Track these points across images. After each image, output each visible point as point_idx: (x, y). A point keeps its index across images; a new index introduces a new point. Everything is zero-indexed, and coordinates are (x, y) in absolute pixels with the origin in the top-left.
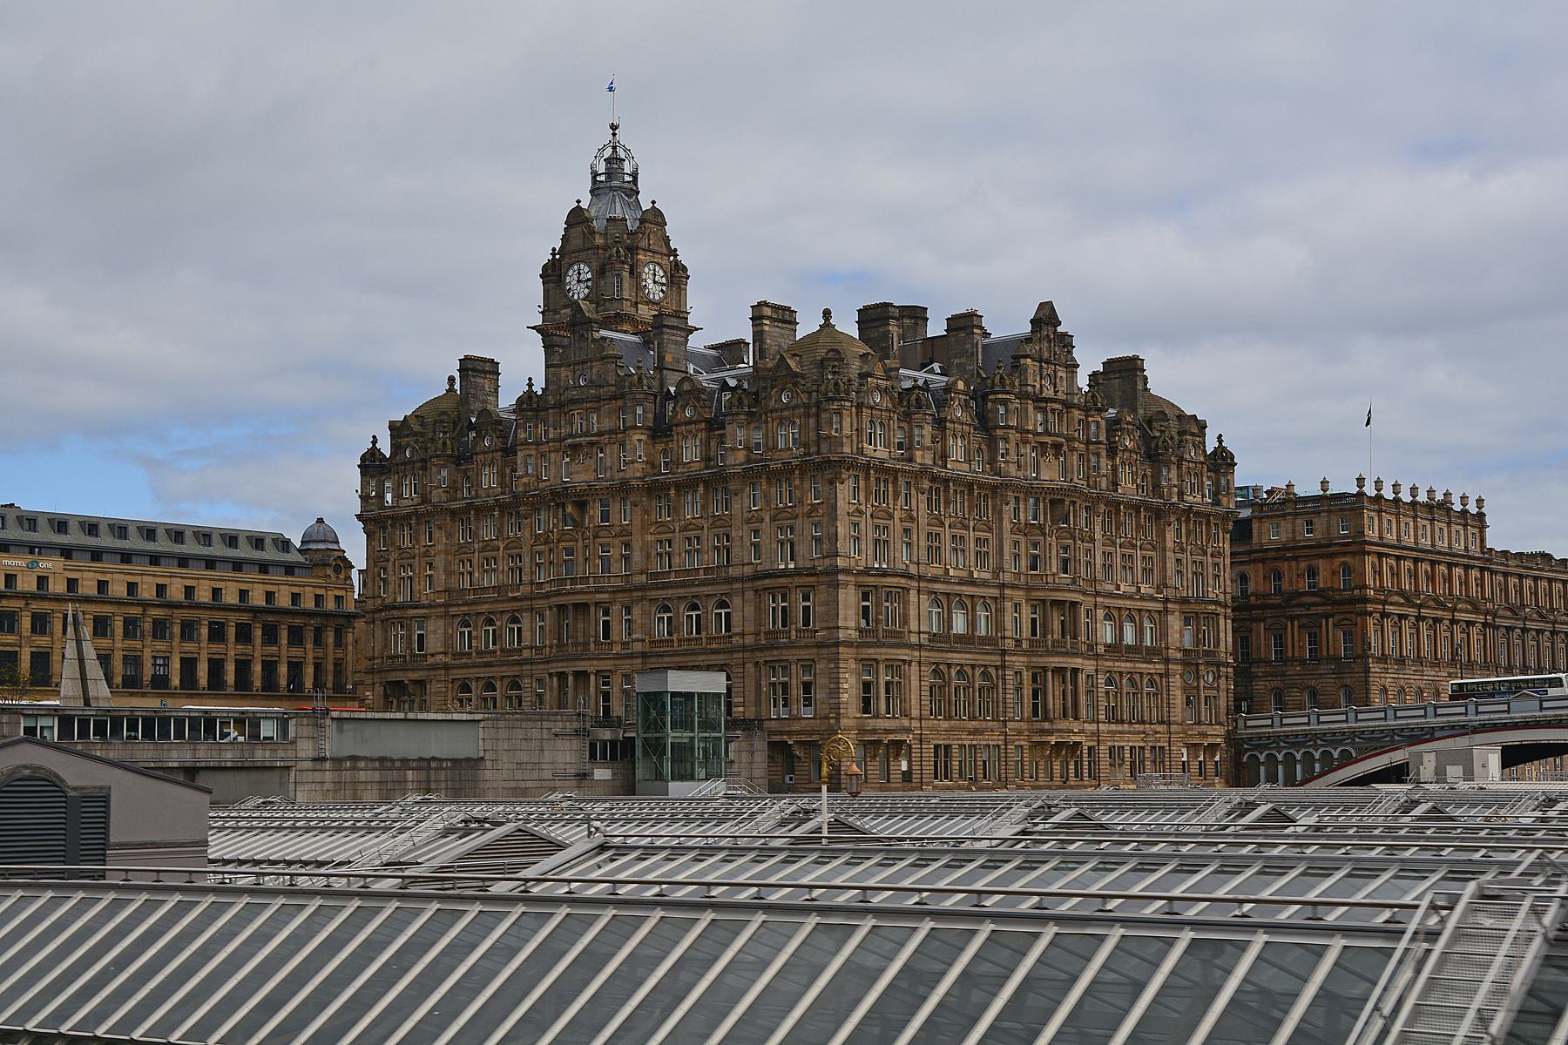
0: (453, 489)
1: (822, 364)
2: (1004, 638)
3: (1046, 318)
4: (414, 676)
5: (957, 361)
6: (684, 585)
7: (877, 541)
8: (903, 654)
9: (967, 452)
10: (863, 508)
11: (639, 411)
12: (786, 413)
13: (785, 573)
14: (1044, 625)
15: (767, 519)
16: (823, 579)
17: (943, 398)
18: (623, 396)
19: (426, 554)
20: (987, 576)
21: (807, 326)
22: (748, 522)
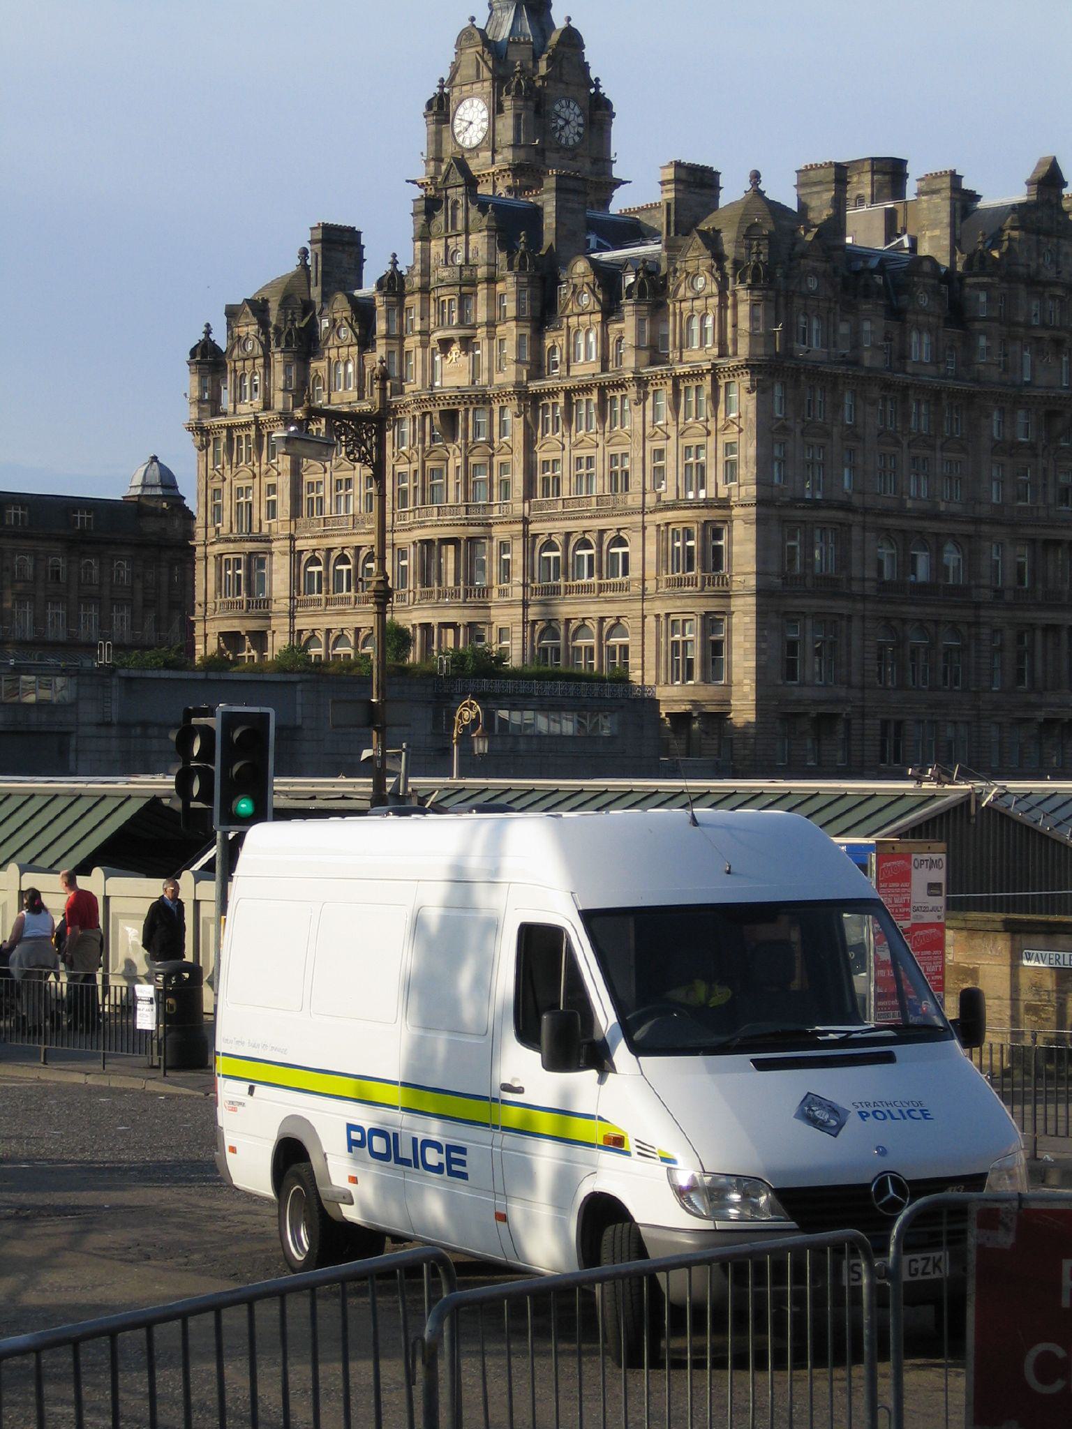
2: (979, 586)
4: (253, 625)
5: (928, 234)
8: (841, 606)
12: (697, 303)
14: (1033, 572)
15: (673, 435)
21: (732, 192)
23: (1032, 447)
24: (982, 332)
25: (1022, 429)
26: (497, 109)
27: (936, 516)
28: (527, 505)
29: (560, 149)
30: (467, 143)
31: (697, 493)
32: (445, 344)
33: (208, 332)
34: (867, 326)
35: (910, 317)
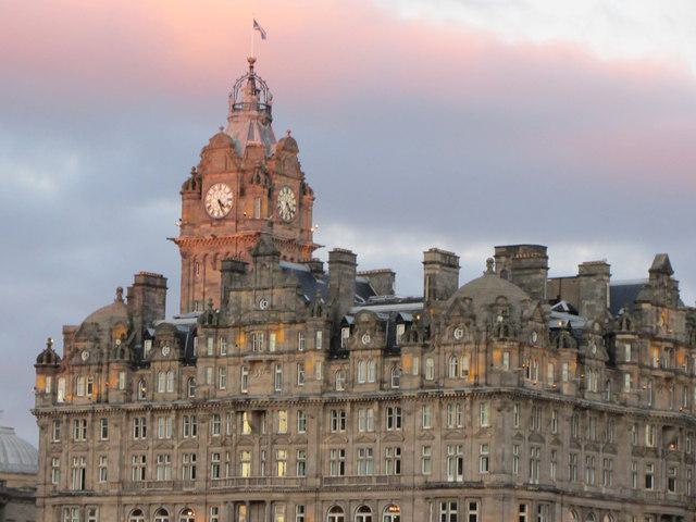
0: (129, 390)
1: (491, 308)
3: (662, 270)
5: (587, 303)
6: (357, 489)
7: (531, 460)
9: (599, 384)
10: (522, 432)
11: (319, 334)
12: (458, 348)
13: (455, 485)
15: (438, 437)
16: (489, 491)
17: (579, 338)
18: (303, 322)
19: (100, 448)
20: (612, 492)
22: (421, 438)
23: (655, 450)
24: (627, 372)
25: (648, 438)
26: (242, 193)
27: (601, 497)
28: (318, 480)
29: (283, 222)
30: (216, 215)
31: (455, 477)
32: (253, 362)
33: (49, 345)
34: (565, 366)
35: (587, 361)
